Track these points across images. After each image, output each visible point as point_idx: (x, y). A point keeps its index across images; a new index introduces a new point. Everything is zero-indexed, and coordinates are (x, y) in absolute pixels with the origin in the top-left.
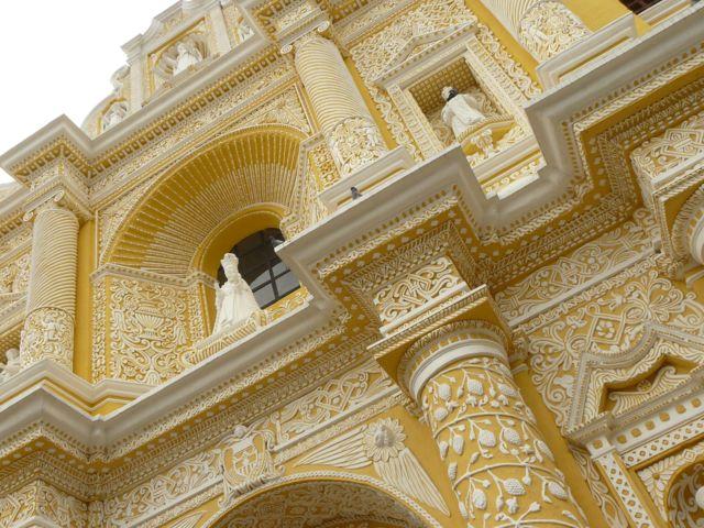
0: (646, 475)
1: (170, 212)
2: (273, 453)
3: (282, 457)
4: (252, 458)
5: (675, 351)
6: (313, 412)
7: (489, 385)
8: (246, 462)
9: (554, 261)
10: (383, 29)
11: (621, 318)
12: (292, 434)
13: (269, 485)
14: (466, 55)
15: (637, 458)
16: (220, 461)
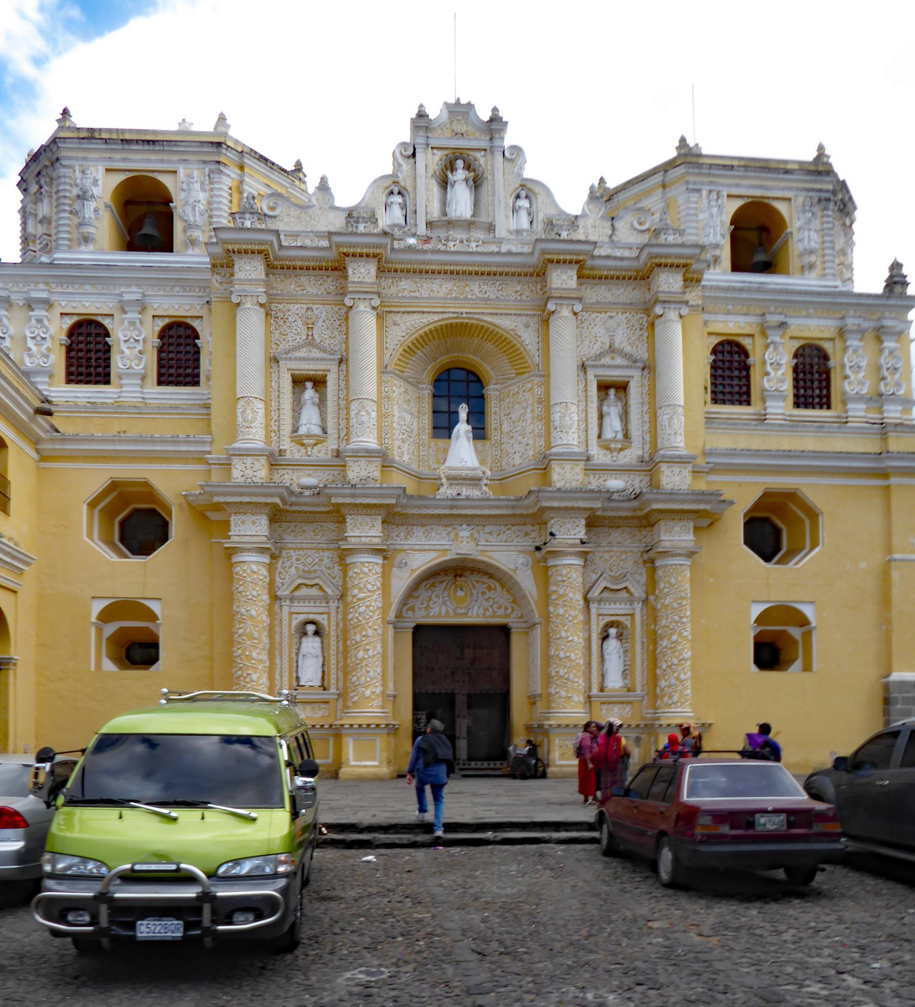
0: (601, 617)
1: (430, 341)
2: (477, 545)
3: (480, 548)
4: (468, 542)
5: (630, 587)
6: (498, 535)
7: (576, 576)
8: (465, 543)
9: (612, 527)
10: (601, 312)
11: (621, 563)
12: (487, 541)
13: (472, 557)
14: (631, 379)
15: (601, 612)
16: (452, 535)
